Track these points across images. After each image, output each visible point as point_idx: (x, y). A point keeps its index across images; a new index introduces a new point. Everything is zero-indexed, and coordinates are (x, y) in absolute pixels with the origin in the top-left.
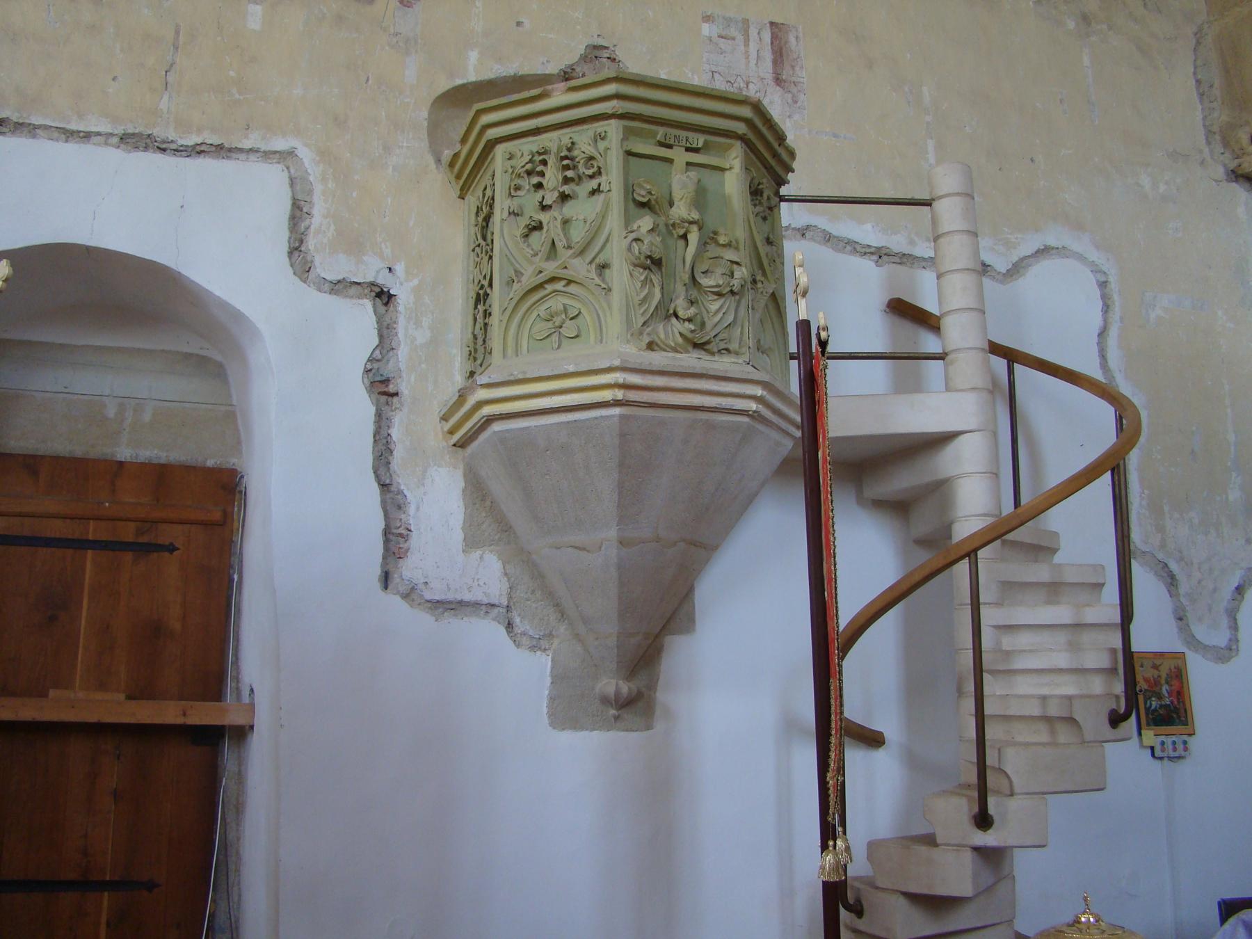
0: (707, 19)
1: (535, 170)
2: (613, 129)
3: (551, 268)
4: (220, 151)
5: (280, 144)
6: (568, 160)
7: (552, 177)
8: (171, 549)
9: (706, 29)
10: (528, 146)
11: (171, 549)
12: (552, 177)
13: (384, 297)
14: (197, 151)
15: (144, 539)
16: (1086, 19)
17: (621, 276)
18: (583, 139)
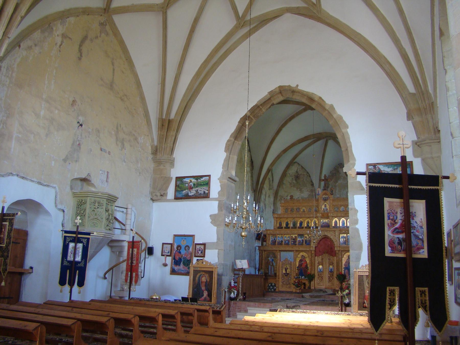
0: (101, 170)
1: (95, 202)
2: (105, 200)
3: (96, 217)
4: (48, 186)
5: (54, 186)
6: (99, 203)
7: (97, 204)
8: (19, 243)
9: (101, 172)
10: (93, 199)
11: (19, 243)
12: (97, 204)
13: (64, 211)
14: (45, 185)
15: (16, 241)
16: (140, 173)
17: (104, 220)
18: (101, 200)
